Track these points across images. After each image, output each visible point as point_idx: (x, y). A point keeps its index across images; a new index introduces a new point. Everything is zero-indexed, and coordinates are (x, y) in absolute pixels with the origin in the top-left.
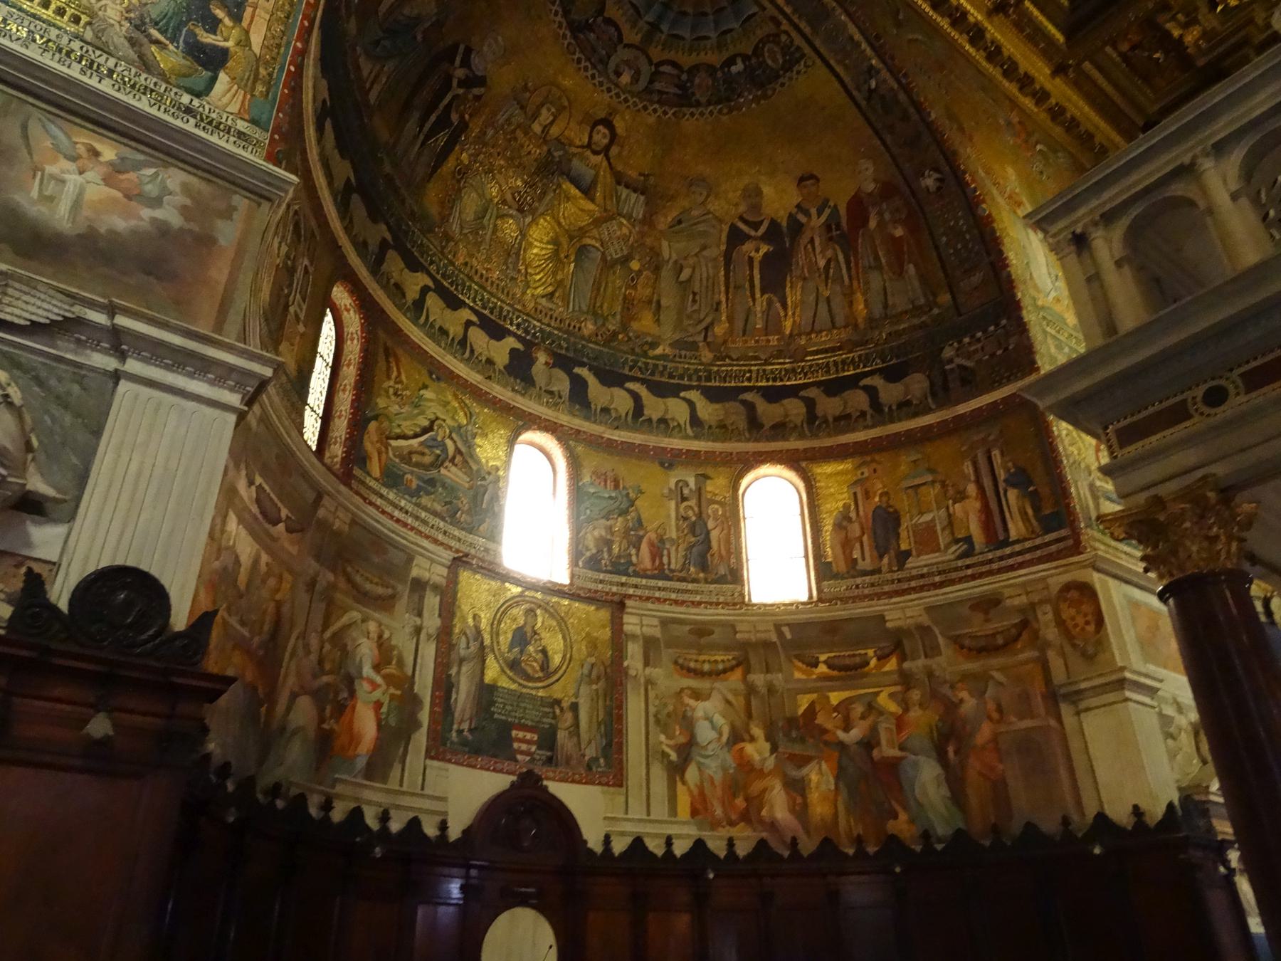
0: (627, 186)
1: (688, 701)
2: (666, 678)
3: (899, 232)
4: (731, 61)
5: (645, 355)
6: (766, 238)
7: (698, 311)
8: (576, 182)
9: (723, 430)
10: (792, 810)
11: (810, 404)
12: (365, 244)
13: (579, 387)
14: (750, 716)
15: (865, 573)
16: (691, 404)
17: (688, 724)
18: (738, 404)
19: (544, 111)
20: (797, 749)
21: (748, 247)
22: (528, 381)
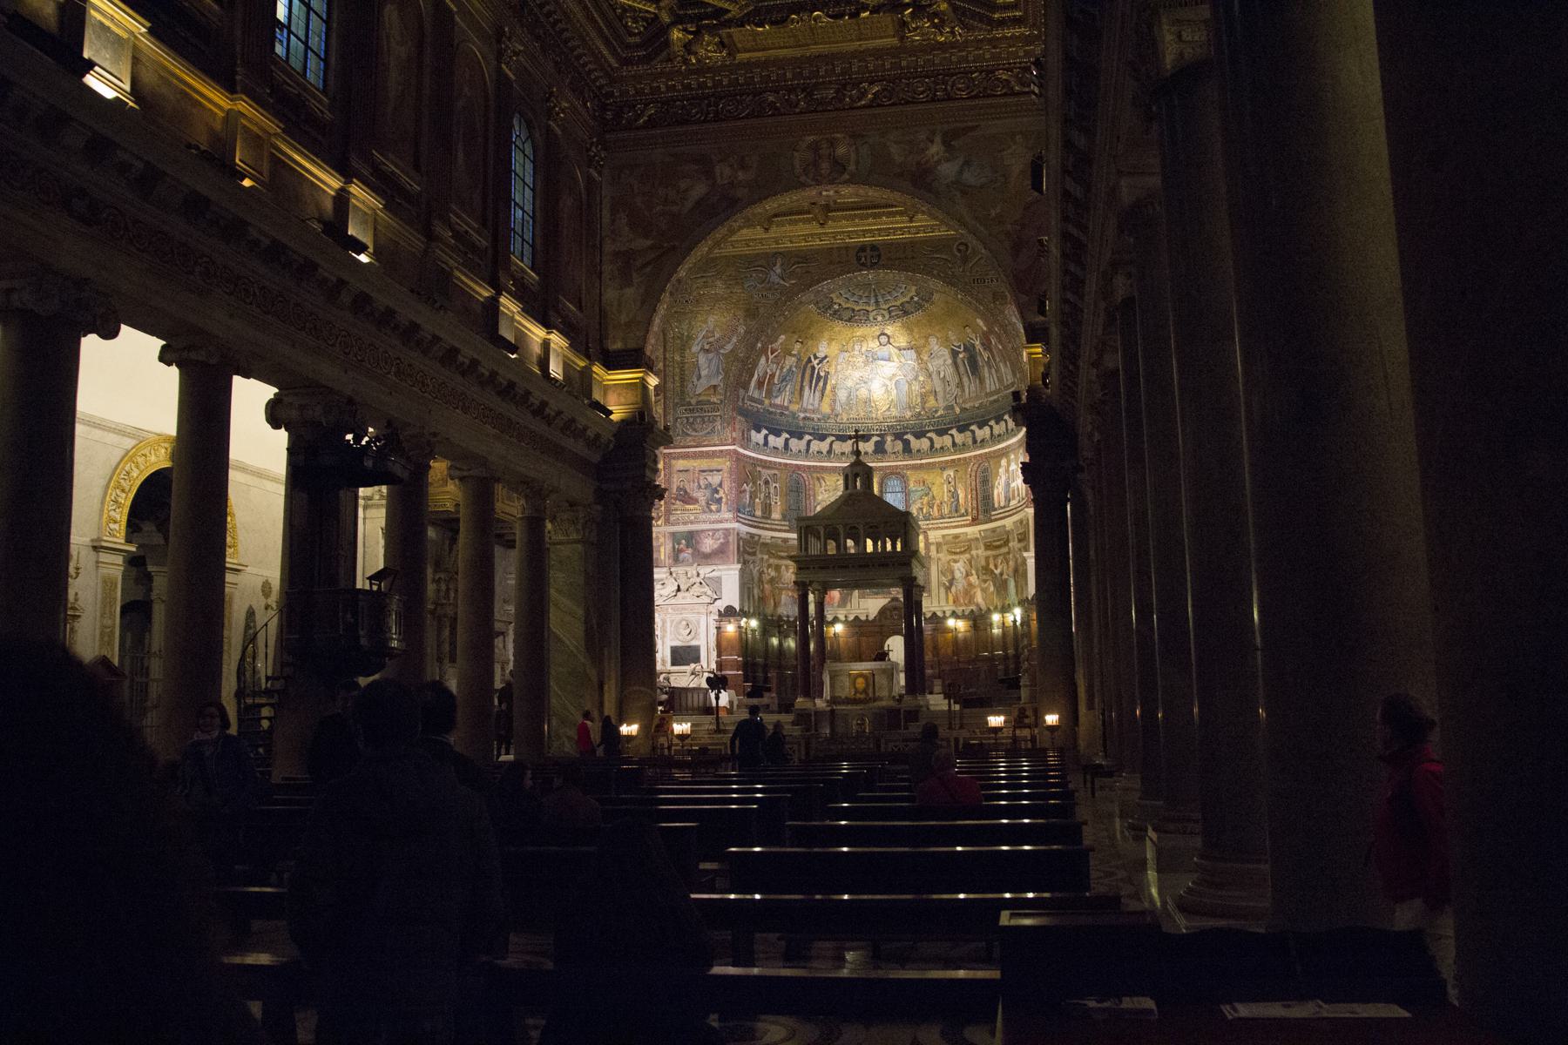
0: (904, 349)
1: (952, 564)
2: (945, 557)
3: (1000, 347)
4: (912, 298)
5: (934, 417)
6: (964, 351)
7: (951, 390)
8: (882, 359)
9: (964, 447)
10: (984, 599)
11: (991, 427)
12: (800, 451)
13: (907, 443)
14: (971, 566)
15: (1002, 508)
16: (952, 436)
17: (952, 572)
18: (969, 433)
19: (856, 346)
20: (984, 577)
21: (961, 356)
22: (884, 452)
